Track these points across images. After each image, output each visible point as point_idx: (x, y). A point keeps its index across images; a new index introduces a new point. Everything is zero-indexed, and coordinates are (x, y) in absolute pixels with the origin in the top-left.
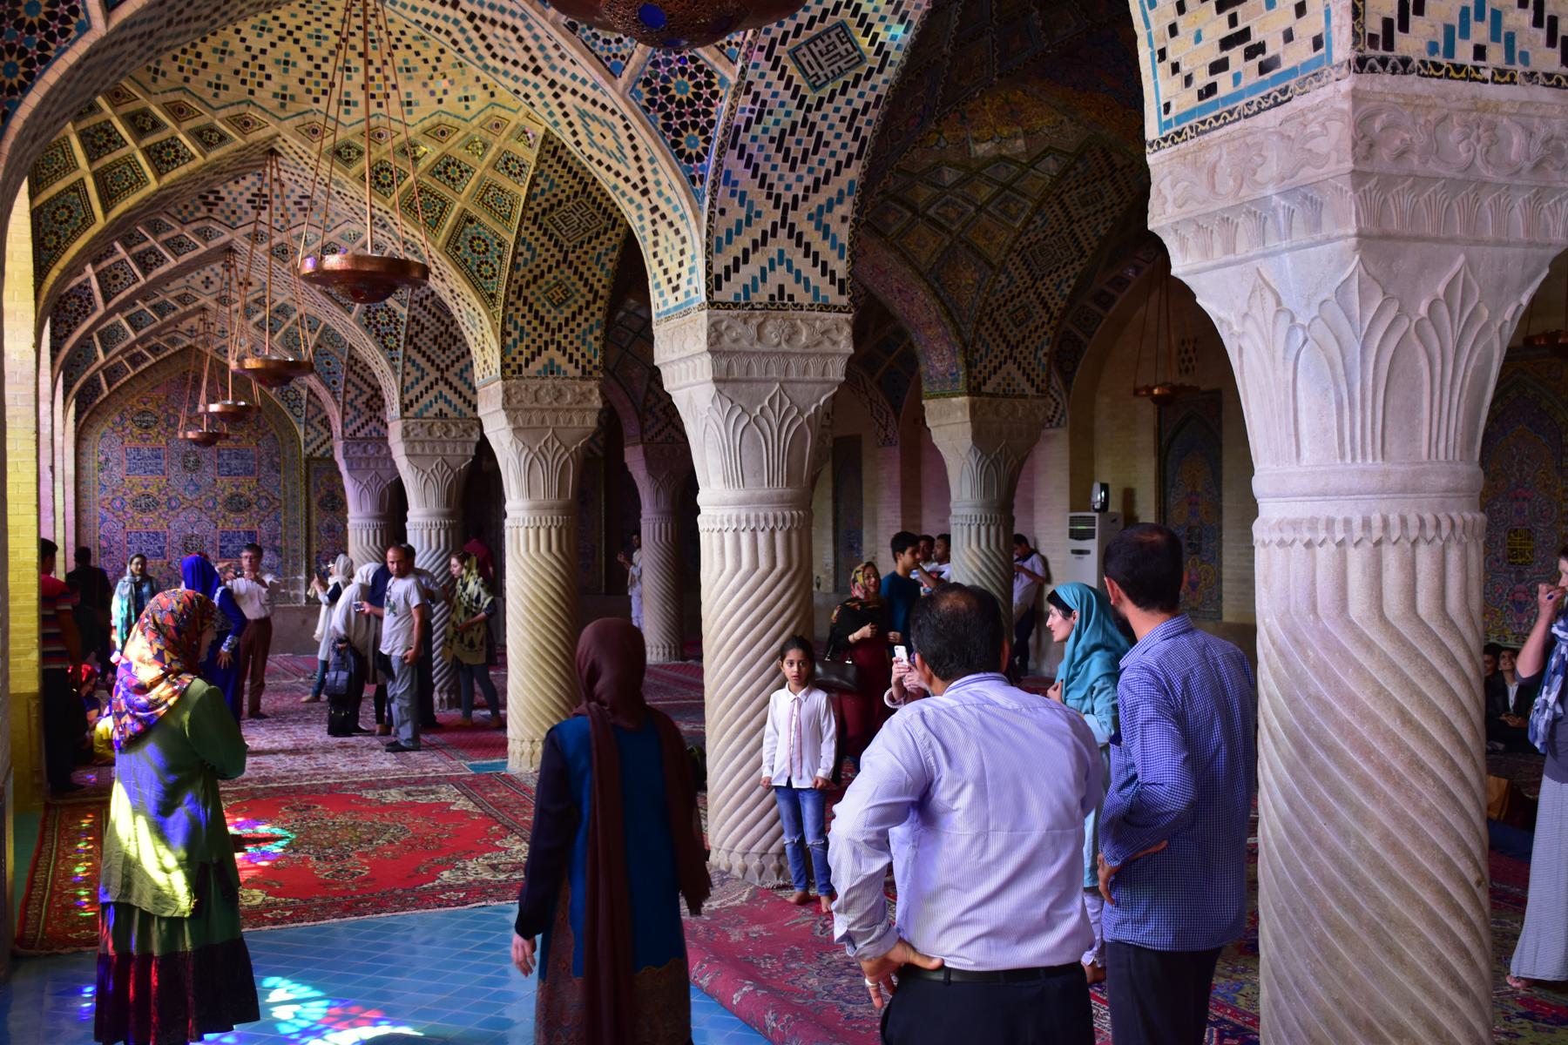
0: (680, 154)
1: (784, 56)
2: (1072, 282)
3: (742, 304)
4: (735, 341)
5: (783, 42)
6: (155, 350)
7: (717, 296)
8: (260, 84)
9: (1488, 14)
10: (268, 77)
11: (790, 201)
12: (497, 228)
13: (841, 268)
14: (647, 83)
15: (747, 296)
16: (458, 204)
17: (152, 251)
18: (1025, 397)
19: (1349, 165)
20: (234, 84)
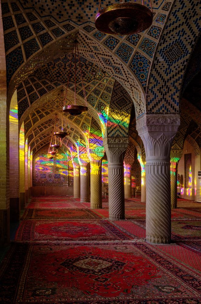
0: (103, 116)
1: (115, 103)
2: (186, 129)
3: (112, 137)
4: (111, 142)
5: (115, 101)
6: (45, 143)
7: (108, 136)
8: (54, 105)
9: (164, 107)
10: (55, 104)
11: (119, 122)
12: (88, 124)
13: (127, 131)
14: (98, 107)
15: (113, 136)
16: (82, 121)
17: (42, 128)
18: (179, 149)
19: (146, 124)
20: (50, 105)
